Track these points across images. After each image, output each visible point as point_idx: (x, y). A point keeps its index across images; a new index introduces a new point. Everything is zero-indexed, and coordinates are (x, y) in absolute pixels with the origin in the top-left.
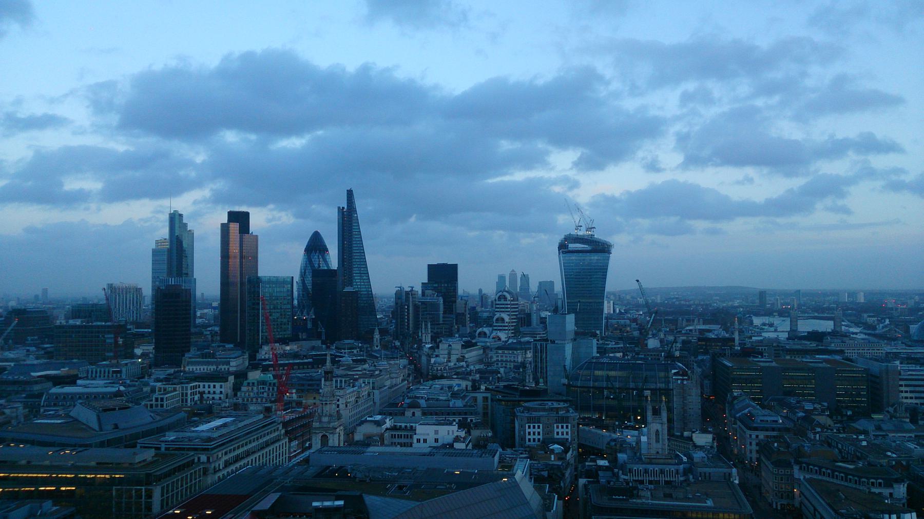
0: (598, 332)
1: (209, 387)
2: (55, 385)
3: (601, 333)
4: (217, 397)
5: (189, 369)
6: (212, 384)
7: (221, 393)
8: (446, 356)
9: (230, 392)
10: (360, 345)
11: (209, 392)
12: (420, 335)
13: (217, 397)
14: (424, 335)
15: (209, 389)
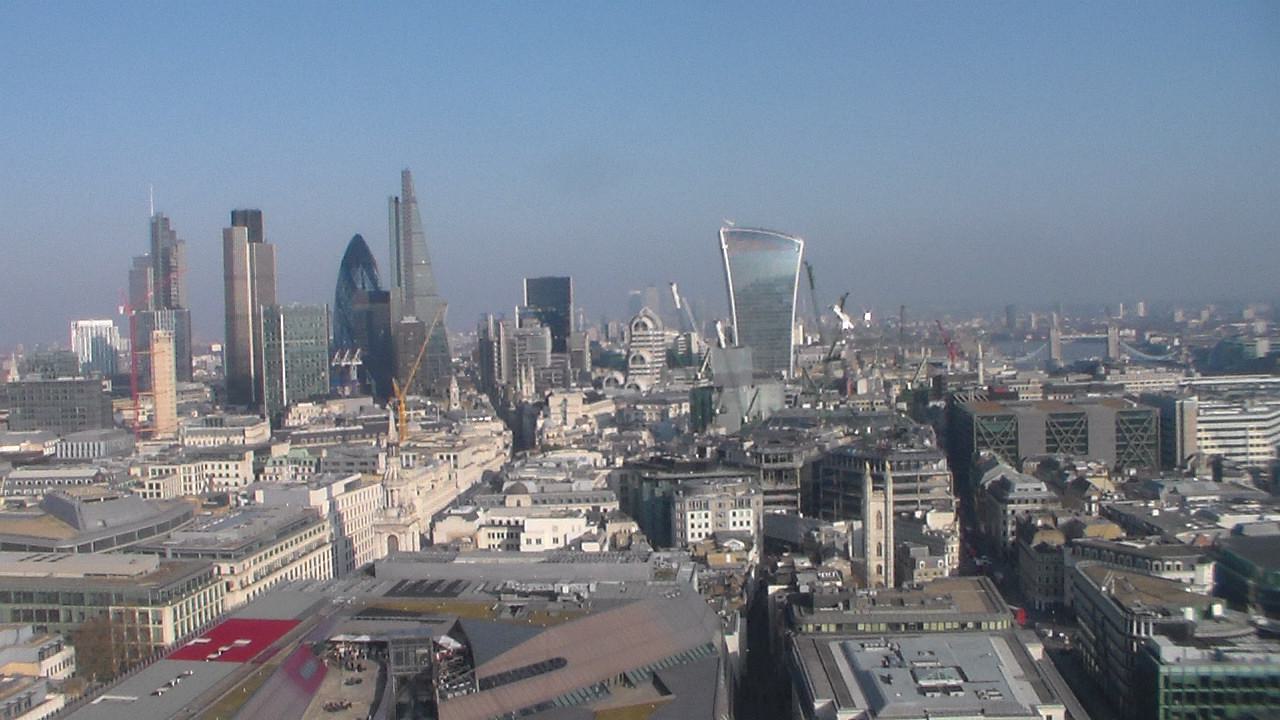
0: (784, 373)
1: (220, 467)
2: (16, 465)
3: (788, 374)
4: (231, 482)
5: (190, 443)
6: (224, 464)
7: (237, 476)
8: (560, 416)
9: (251, 477)
10: (429, 403)
11: (220, 475)
12: (518, 385)
13: (231, 482)
14: (524, 386)
15: (220, 471)
